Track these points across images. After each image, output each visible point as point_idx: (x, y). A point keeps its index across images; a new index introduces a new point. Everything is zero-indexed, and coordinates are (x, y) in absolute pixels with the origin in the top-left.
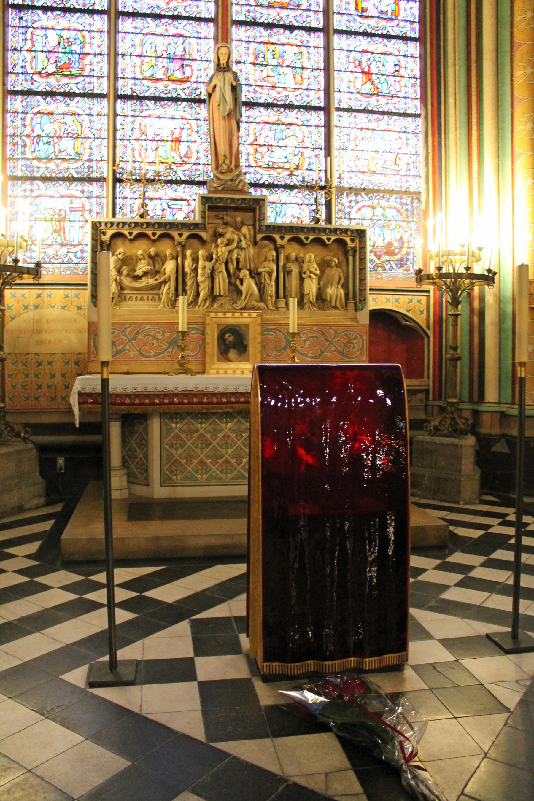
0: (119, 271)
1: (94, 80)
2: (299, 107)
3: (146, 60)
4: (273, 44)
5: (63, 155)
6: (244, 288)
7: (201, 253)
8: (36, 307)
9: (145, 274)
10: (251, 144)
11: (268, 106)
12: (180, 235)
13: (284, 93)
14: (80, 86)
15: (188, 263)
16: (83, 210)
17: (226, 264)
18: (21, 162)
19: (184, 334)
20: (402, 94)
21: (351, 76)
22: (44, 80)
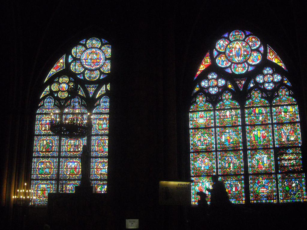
3: (69, 147)
4: (103, 140)
10: (96, 168)
11: (100, 157)
14: (51, 154)
18: (35, 175)
22: (42, 153)
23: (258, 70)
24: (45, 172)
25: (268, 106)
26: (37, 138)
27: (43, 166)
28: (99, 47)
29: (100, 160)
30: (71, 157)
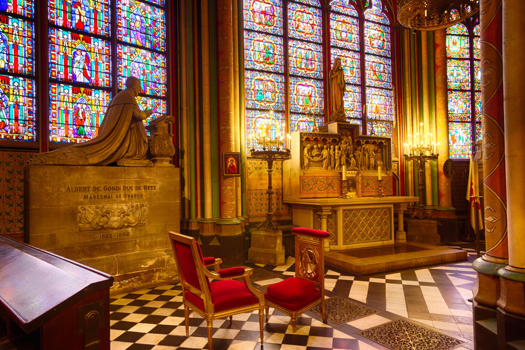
1: (279, 66)
2: (352, 84)
3: (298, 59)
5: (267, 100)
6: (352, 162)
7: (336, 147)
8: (260, 168)
9: (316, 155)
12: (329, 139)
18: (250, 102)
24: (266, 98)
26: (249, 35)
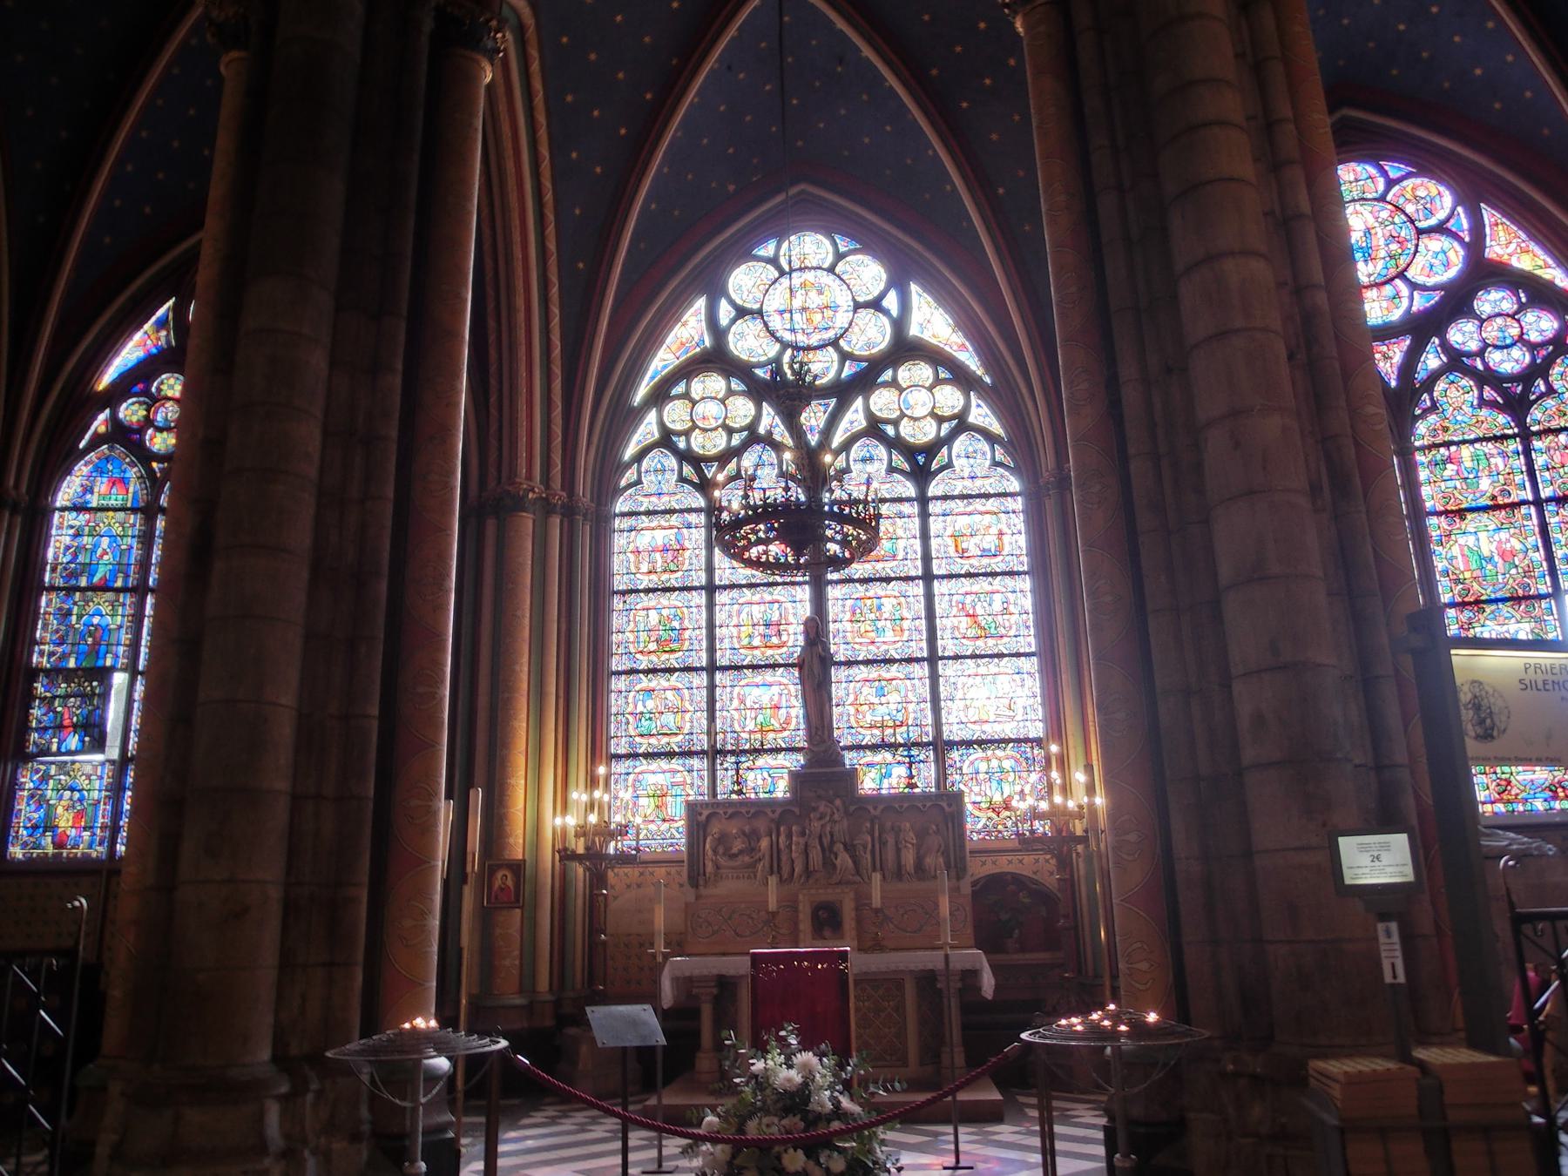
0: (715, 851)
2: (900, 661)
6: (838, 862)
8: (639, 886)
9: (741, 852)
11: (867, 662)
13: (885, 647)
15: (782, 839)
16: (684, 783)
17: (820, 838)
19: (774, 914)
20: (1012, 633)
21: (955, 621)
23: (1456, 301)
25: (1514, 436)
27: (650, 704)
28: (826, 265)
29: (862, 672)
30: (754, 667)
